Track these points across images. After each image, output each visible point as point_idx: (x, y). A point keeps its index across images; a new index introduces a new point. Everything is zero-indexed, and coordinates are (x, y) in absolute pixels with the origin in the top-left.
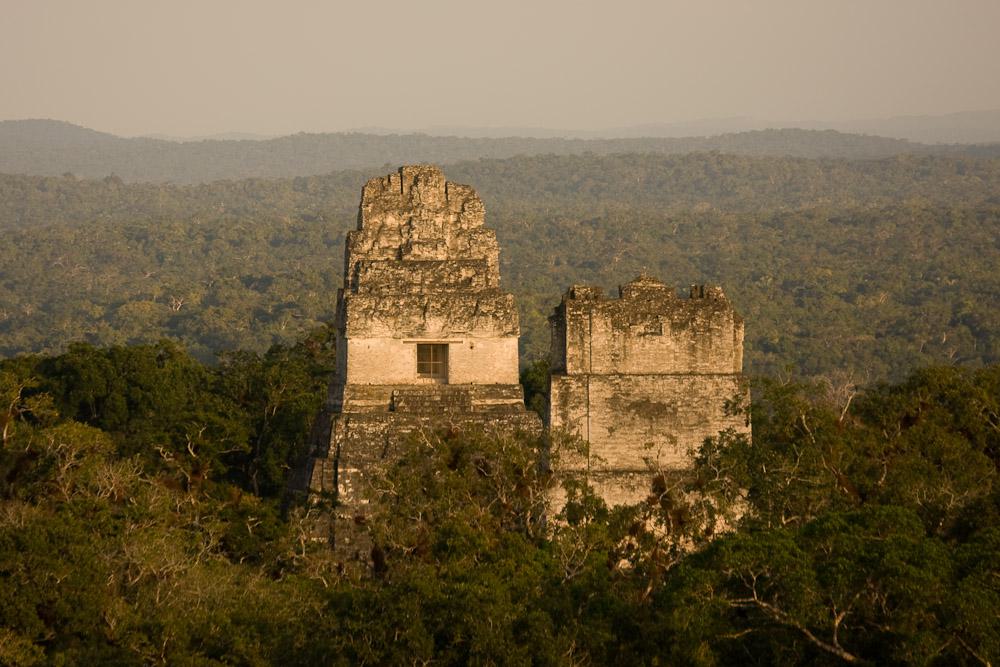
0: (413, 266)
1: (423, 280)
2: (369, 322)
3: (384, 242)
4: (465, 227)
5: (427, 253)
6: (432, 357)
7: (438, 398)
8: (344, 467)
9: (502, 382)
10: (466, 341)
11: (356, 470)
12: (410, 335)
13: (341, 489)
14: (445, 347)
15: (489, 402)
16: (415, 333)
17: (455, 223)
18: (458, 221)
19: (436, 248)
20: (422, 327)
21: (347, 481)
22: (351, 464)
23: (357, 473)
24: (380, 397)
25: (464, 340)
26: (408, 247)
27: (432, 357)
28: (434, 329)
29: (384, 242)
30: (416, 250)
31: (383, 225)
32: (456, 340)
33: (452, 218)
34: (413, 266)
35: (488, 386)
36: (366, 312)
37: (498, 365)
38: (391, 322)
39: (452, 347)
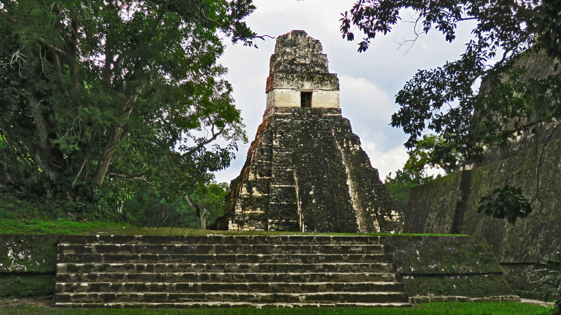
0: (297, 65)
1: (302, 70)
3: (285, 58)
4: (316, 53)
5: (302, 61)
6: (306, 97)
7: (309, 112)
8: (276, 134)
13: (274, 143)
15: (328, 115)
17: (312, 52)
18: (313, 51)
19: (305, 59)
20: (303, 85)
26: (294, 59)
29: (285, 58)
30: (298, 60)
33: (311, 50)
34: (297, 65)
36: (281, 78)
39: (314, 94)
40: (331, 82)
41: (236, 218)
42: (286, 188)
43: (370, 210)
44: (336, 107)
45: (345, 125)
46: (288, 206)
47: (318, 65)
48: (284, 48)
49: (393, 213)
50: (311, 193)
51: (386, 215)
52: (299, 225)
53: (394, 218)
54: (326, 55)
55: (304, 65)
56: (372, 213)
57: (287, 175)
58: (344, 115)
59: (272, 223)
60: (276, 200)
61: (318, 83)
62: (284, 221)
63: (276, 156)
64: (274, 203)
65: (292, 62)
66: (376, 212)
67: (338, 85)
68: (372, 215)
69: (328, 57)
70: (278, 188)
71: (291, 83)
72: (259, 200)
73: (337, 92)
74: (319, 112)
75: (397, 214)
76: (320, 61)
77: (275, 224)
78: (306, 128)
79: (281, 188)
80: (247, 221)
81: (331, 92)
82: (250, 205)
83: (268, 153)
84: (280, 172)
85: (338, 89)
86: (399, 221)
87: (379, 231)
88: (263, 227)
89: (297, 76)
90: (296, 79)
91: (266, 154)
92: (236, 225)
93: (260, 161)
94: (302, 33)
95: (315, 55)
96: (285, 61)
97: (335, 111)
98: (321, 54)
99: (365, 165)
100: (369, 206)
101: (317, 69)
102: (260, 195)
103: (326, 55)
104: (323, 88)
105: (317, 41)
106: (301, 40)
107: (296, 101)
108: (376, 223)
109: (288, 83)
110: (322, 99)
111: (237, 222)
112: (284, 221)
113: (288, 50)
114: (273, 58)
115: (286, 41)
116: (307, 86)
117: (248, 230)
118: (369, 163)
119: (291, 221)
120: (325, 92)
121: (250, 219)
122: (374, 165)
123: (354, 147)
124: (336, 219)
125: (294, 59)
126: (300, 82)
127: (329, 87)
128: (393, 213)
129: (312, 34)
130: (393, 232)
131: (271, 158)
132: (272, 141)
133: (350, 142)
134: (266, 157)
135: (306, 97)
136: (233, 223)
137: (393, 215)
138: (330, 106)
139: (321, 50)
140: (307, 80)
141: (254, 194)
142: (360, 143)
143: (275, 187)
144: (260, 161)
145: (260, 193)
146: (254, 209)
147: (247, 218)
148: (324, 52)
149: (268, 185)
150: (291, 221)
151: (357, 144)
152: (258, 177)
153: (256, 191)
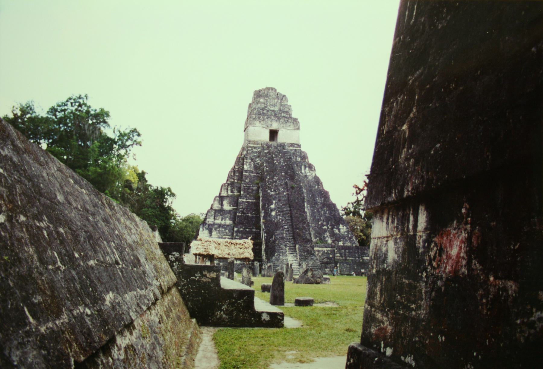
0: (268, 111)
3: (259, 105)
5: (272, 109)
6: (273, 134)
9: (295, 143)
10: (284, 130)
20: (271, 125)
24: (258, 144)
27: (273, 134)
28: (275, 126)
29: (259, 105)
30: (269, 107)
31: (259, 101)
33: (279, 101)
36: (254, 119)
38: (262, 122)
41: (207, 226)
43: (322, 224)
45: (304, 157)
47: (284, 112)
48: (259, 99)
49: (341, 226)
50: (273, 206)
52: (260, 234)
53: (342, 230)
55: (274, 111)
56: (324, 225)
58: (303, 149)
60: (243, 212)
62: (247, 230)
65: (263, 109)
71: (262, 122)
72: (229, 212)
74: (283, 146)
75: (345, 227)
76: (286, 110)
78: (272, 156)
79: (248, 202)
80: (216, 229)
84: (248, 189)
85: (298, 129)
89: (267, 118)
91: (237, 174)
93: (232, 180)
96: (259, 108)
97: (296, 146)
99: (318, 188)
101: (283, 115)
105: (284, 96)
106: (272, 93)
107: (265, 136)
112: (247, 230)
113: (262, 100)
114: (250, 106)
118: (322, 186)
119: (254, 230)
120: (289, 131)
122: (326, 187)
125: (266, 107)
127: (292, 127)
128: (341, 226)
129: (281, 90)
130: (341, 243)
131: (242, 178)
133: (307, 169)
136: (203, 230)
138: (292, 142)
139: (287, 101)
143: (243, 202)
144: (232, 180)
147: (216, 226)
148: (289, 103)
150: (254, 230)
152: (230, 193)
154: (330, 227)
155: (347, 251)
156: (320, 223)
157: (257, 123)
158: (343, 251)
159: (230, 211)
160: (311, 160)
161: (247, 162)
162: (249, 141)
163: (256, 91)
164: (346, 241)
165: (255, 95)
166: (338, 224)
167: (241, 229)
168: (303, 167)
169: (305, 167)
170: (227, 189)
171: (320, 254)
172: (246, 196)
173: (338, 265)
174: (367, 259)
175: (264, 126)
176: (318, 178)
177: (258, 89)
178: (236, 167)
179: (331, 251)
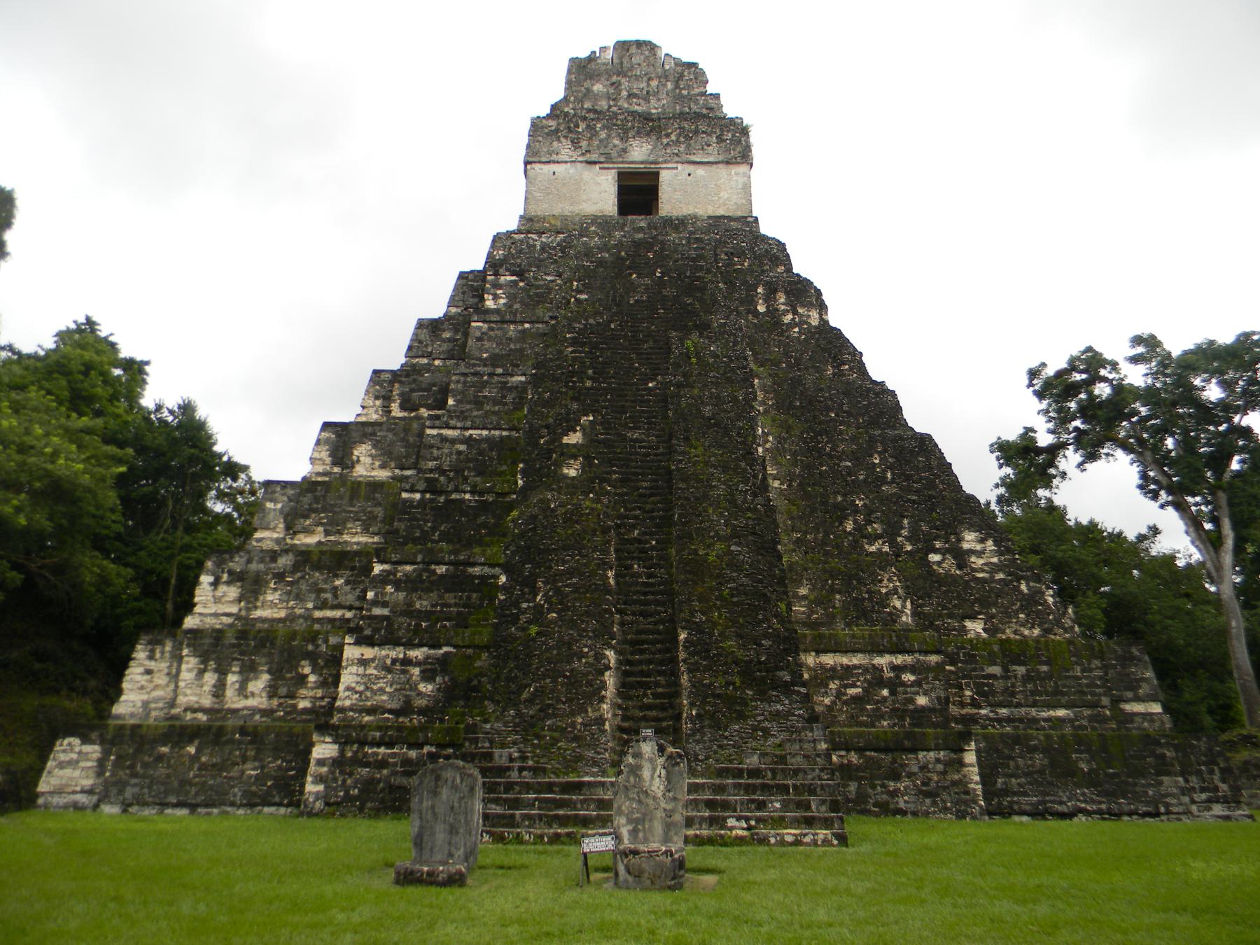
2: (555, 144)
6: (638, 192)
8: (496, 274)
11: (514, 278)
12: (609, 159)
13: (490, 304)
14: (657, 174)
16: (614, 154)
18: (677, 86)
20: (625, 150)
21: (499, 292)
22: (507, 270)
23: (515, 282)
25: (680, 166)
32: (670, 165)
33: (670, 86)
35: (709, 217)
37: (724, 195)
39: (665, 176)
40: (720, 139)
41: (237, 564)
42: (487, 440)
43: (859, 528)
44: (739, 214)
46: (484, 507)
49: (970, 540)
50: (574, 438)
51: (936, 551)
54: (717, 96)
56: (872, 539)
57: (509, 399)
58: (767, 228)
59: (384, 579)
60: (432, 487)
61: (678, 142)
63: (479, 339)
64: (418, 496)
66: (890, 534)
67: (748, 148)
68: (873, 549)
69: (723, 100)
70: (453, 441)
71: (584, 144)
73: (743, 168)
74: (678, 224)
75: (990, 545)
77: (398, 585)
79: (469, 441)
80: (280, 577)
81: (722, 171)
82: (316, 511)
83: (456, 331)
84: (484, 385)
85: (745, 157)
86: (1001, 576)
87: (907, 619)
88: (350, 599)
90: (603, 135)
91: (447, 335)
92: (233, 592)
93: (425, 361)
94: (648, 47)
95: (683, 96)
98: (704, 94)
99: (839, 374)
100: (856, 511)
102: (383, 474)
103: (717, 96)
104: (693, 158)
108: (889, 582)
109: (575, 144)
110: (688, 190)
111: (236, 578)
113: (598, 87)
115: (593, 65)
116: (639, 152)
117: (282, 614)
119: (476, 570)
120: (700, 171)
121: (296, 567)
123: (795, 313)
124: (664, 544)
126: (616, 142)
127: (713, 153)
128: (970, 540)
129: (676, 45)
130: (976, 627)
132: (482, 299)
133: (782, 298)
134: (445, 347)
135: (638, 192)
136: (215, 584)
137: (972, 552)
138: (721, 212)
140: (638, 133)
141: (360, 471)
142: (822, 307)
143: (444, 439)
144: (425, 361)
145: (383, 467)
146: (336, 526)
147: (285, 561)
148: (710, 89)
149: (421, 434)
150: (476, 570)
151: (810, 306)
152: (396, 412)
153: (366, 460)
154: (909, 548)
155: (1021, 670)
156: (849, 526)
157: (565, 149)
158: (996, 670)
159: (375, 486)
160: (801, 266)
161: (496, 286)
162: (530, 220)
163: (573, 61)
164: (1008, 615)
165: (569, 72)
166: (951, 530)
167: (409, 568)
168: (760, 290)
169: (772, 291)
170: (387, 398)
171: (852, 691)
172: (462, 416)
173: (970, 757)
174: (1148, 716)
175: (594, 157)
176: (837, 334)
177: (583, 54)
178: (453, 310)
179: (913, 669)
